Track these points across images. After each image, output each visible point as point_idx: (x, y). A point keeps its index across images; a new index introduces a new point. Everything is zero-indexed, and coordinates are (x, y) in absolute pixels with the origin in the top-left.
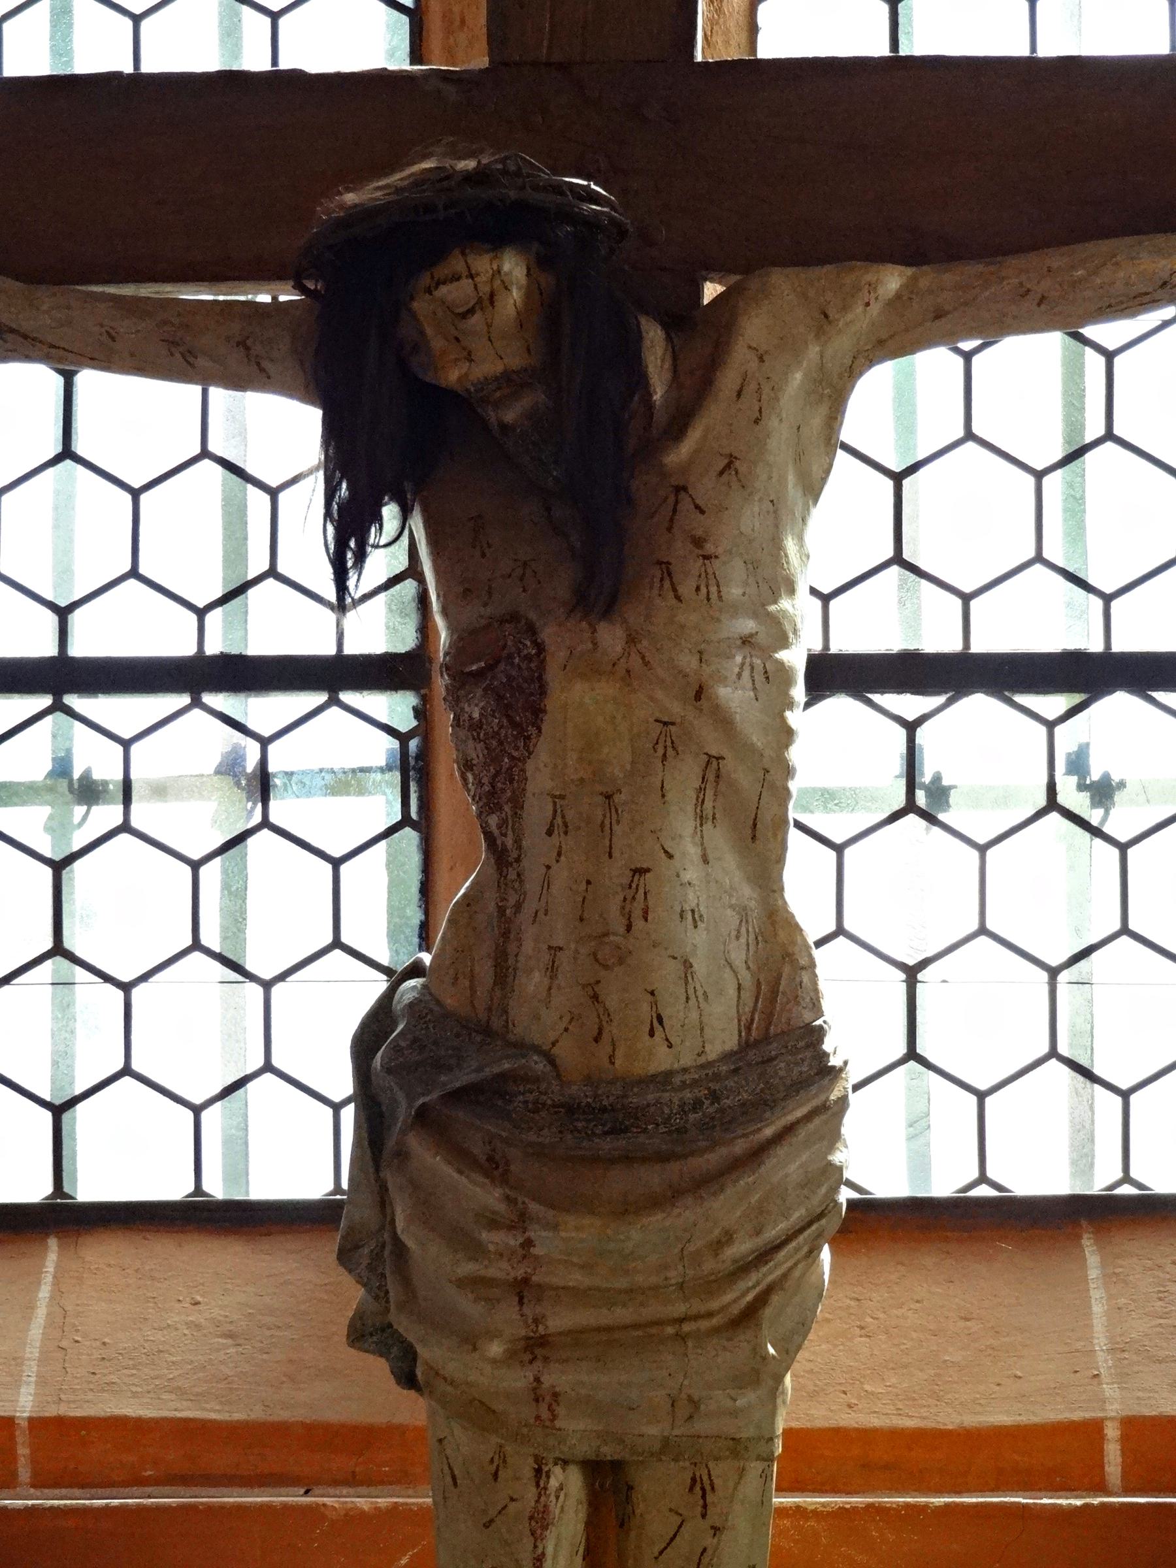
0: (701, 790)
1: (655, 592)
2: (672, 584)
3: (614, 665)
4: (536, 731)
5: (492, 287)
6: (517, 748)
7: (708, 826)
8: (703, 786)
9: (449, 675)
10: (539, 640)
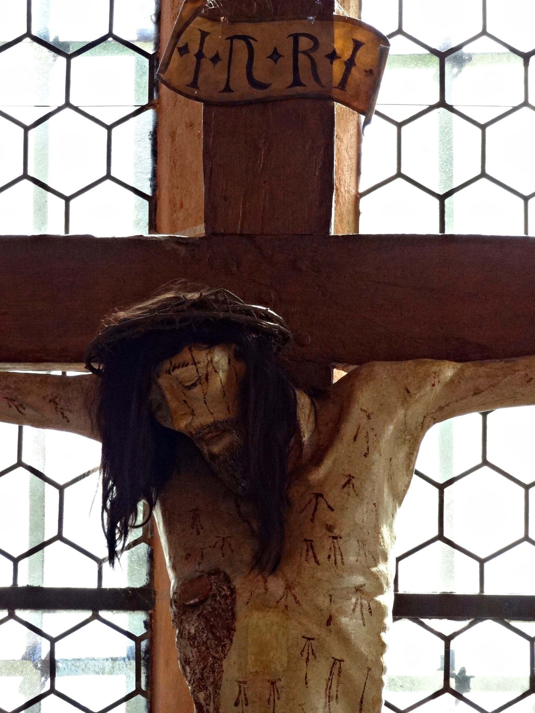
0: (330, 680)
1: (303, 559)
2: (314, 553)
3: (277, 602)
4: (229, 642)
5: (207, 371)
6: (217, 652)
7: (333, 703)
8: (331, 678)
9: (176, 606)
10: (232, 587)
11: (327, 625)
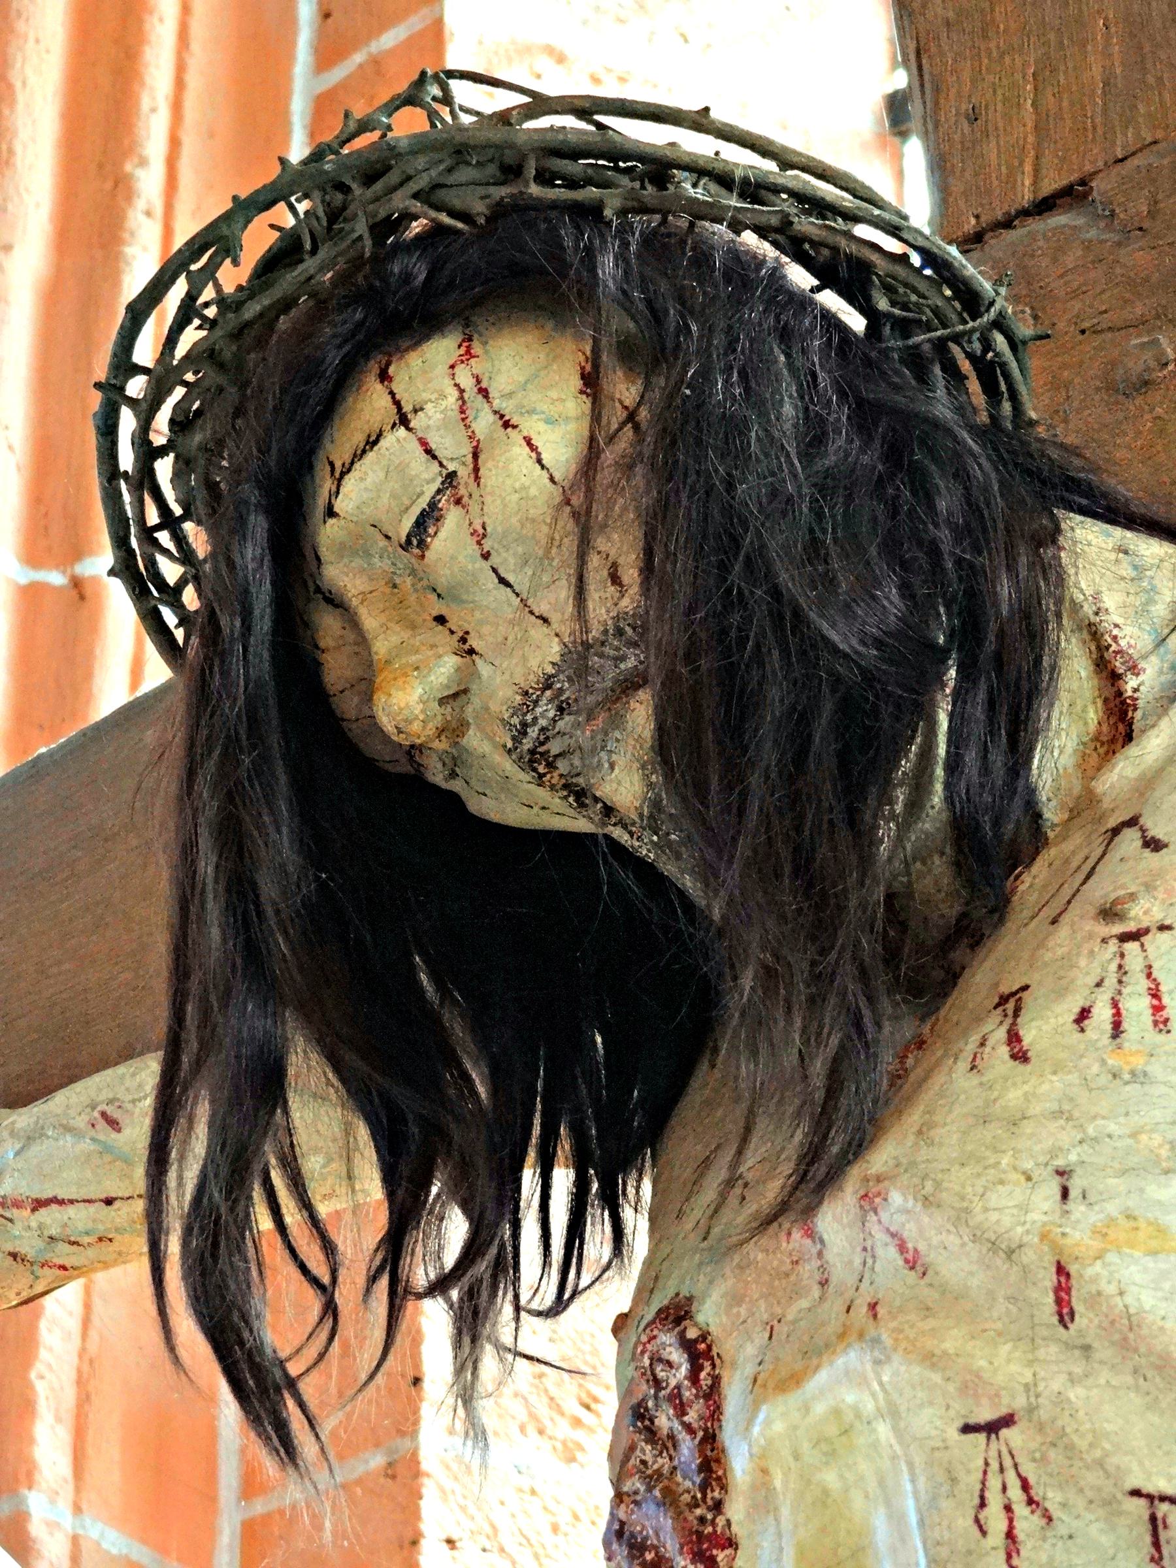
1: (963, 1065)
11: (1062, 1320)
